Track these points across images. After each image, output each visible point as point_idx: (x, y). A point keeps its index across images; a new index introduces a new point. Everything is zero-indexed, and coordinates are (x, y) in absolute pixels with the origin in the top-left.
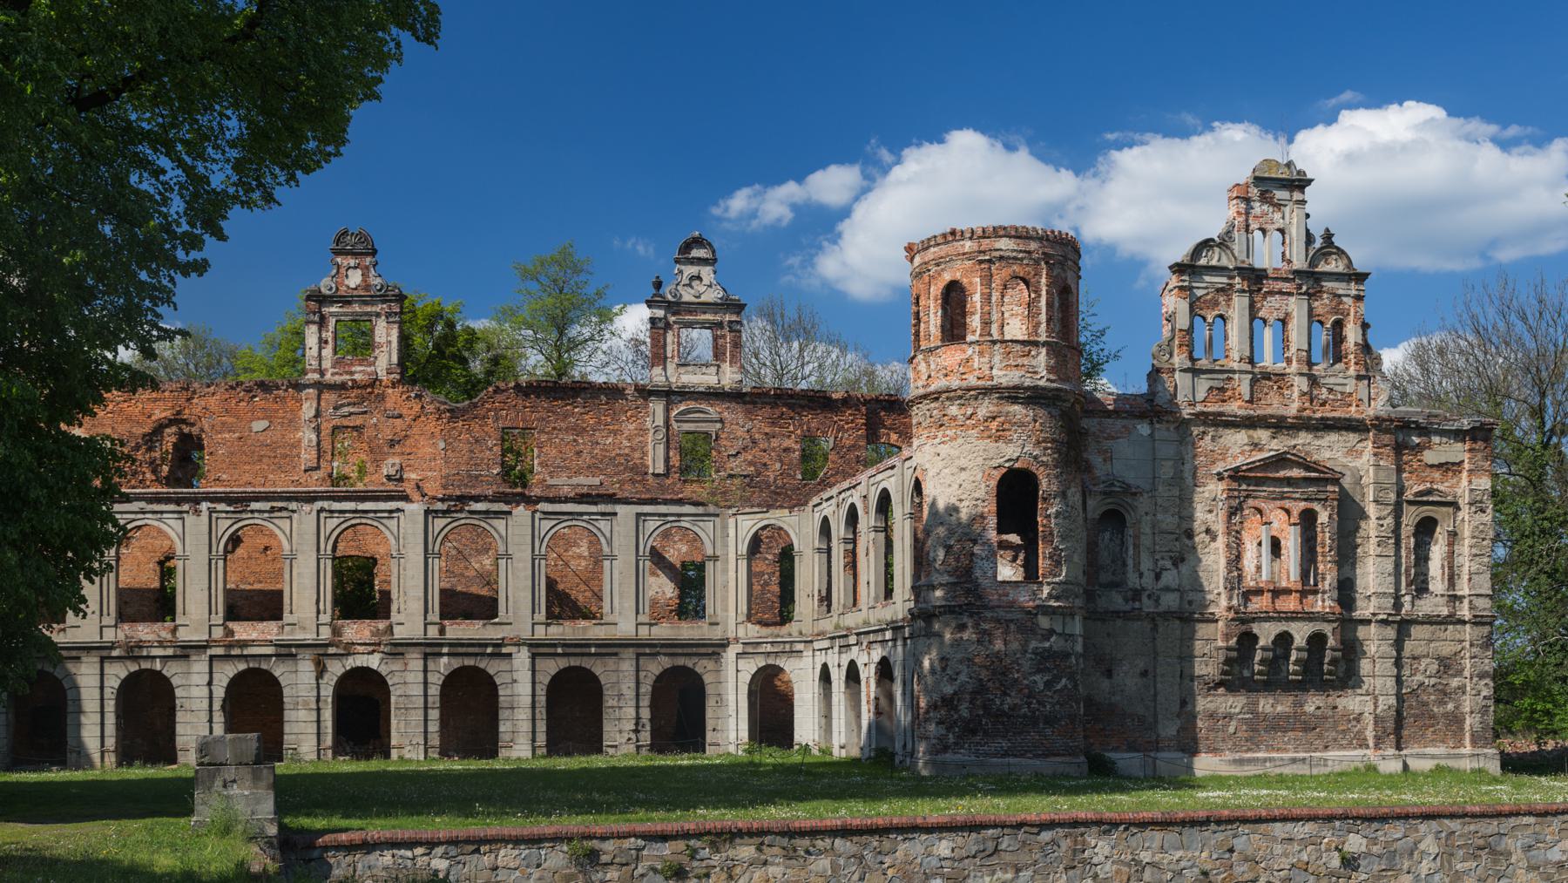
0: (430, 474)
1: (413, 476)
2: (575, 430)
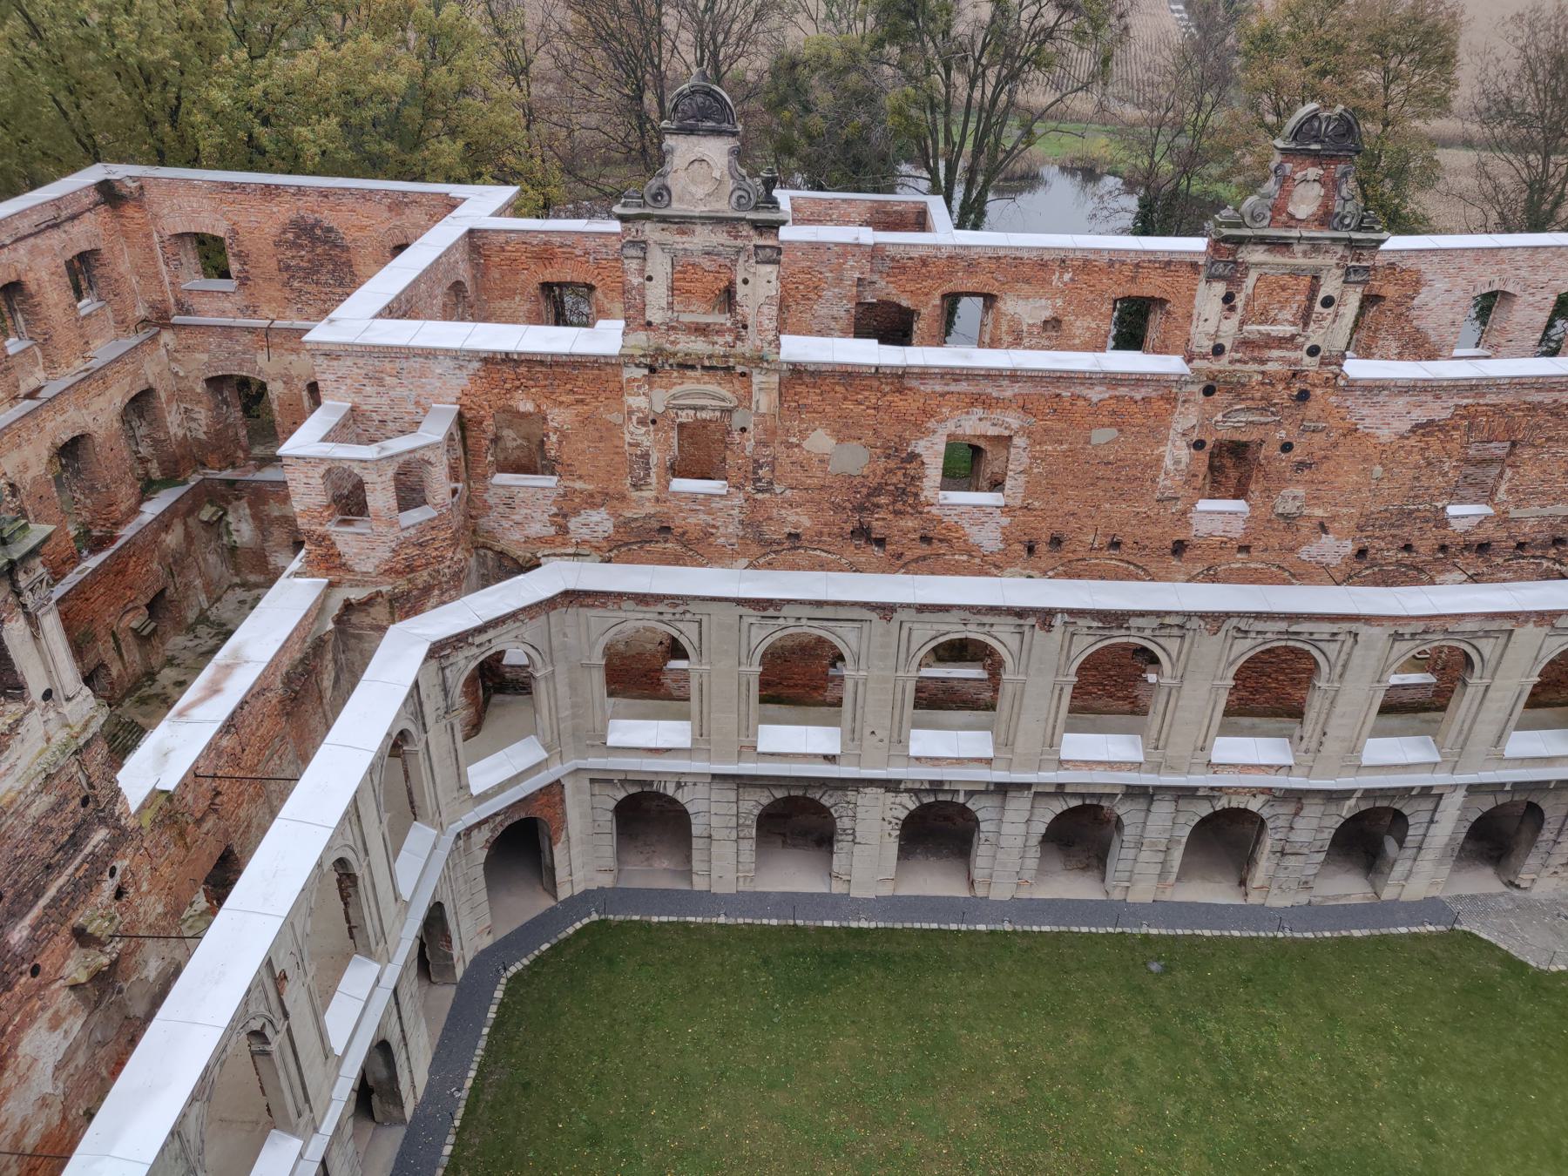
0: (1345, 510)
1: (1319, 512)
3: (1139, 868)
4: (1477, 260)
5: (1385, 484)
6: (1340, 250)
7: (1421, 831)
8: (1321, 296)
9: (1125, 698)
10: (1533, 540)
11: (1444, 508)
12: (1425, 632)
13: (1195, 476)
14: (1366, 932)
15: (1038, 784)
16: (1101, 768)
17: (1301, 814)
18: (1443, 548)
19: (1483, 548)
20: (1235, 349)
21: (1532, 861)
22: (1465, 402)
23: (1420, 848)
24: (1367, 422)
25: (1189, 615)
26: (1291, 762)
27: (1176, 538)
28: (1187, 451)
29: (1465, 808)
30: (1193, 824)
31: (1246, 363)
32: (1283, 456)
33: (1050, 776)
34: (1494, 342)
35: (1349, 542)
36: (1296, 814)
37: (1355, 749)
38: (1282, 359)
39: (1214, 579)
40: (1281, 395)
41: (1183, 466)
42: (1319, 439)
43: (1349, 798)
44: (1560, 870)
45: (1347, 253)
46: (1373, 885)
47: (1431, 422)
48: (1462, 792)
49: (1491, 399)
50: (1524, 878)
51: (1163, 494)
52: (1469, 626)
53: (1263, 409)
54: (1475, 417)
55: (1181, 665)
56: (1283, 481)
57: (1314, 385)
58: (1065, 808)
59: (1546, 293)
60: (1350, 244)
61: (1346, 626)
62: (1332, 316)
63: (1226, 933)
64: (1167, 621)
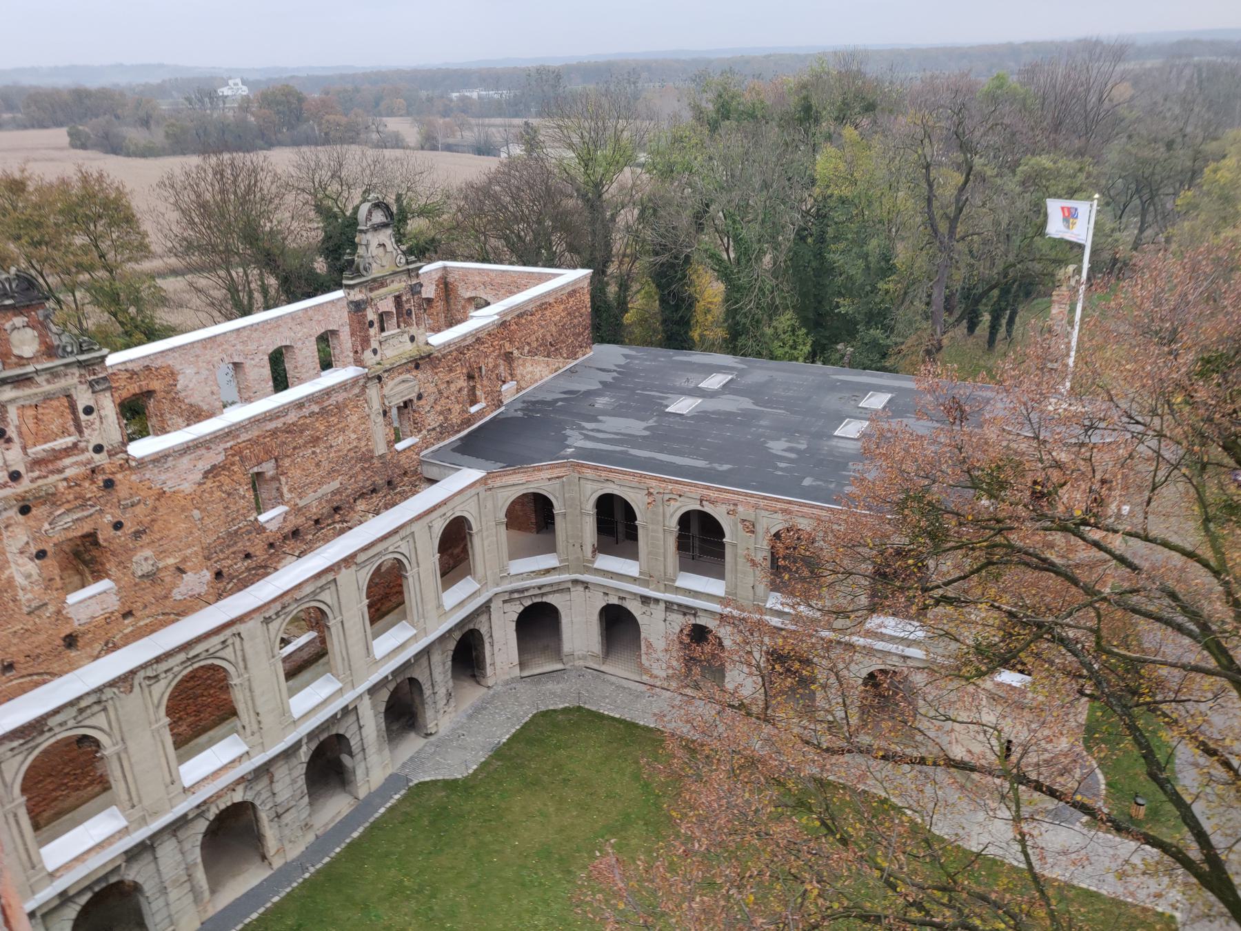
0: (189, 551)
1: (171, 561)
2: (311, 442)
3: (173, 909)
4: (205, 348)
5: (207, 521)
6: (76, 371)
7: (358, 738)
8: (80, 408)
9: (91, 783)
10: (322, 514)
11: (256, 520)
12: (283, 608)
13: (51, 580)
14: (361, 829)
15: (40, 907)
16: (93, 853)
17: (275, 779)
18: (271, 545)
19: (295, 533)
20: (30, 469)
21: (429, 713)
22: (229, 445)
23: (364, 750)
24: (169, 483)
25: (99, 690)
26: (246, 748)
27: (63, 635)
28: (32, 564)
29: (374, 706)
30: (199, 843)
31: (45, 477)
32: (119, 533)
33: (48, 893)
34: (246, 396)
35: (205, 571)
36: (272, 782)
37: (285, 711)
38: (75, 463)
39: (116, 647)
40: (90, 490)
41: (35, 577)
42: (139, 510)
43: (300, 747)
44: (446, 709)
45: (83, 372)
46: (351, 793)
47: (214, 467)
48: (367, 697)
49: (244, 437)
50: (431, 727)
51: (29, 606)
52: (308, 589)
53: (81, 505)
54: (241, 452)
55: (116, 731)
56: (129, 552)
57: (113, 473)
58: (78, 908)
59: (260, 356)
60: (80, 364)
61: (228, 632)
62: (98, 419)
63: (269, 905)
64: (83, 704)
